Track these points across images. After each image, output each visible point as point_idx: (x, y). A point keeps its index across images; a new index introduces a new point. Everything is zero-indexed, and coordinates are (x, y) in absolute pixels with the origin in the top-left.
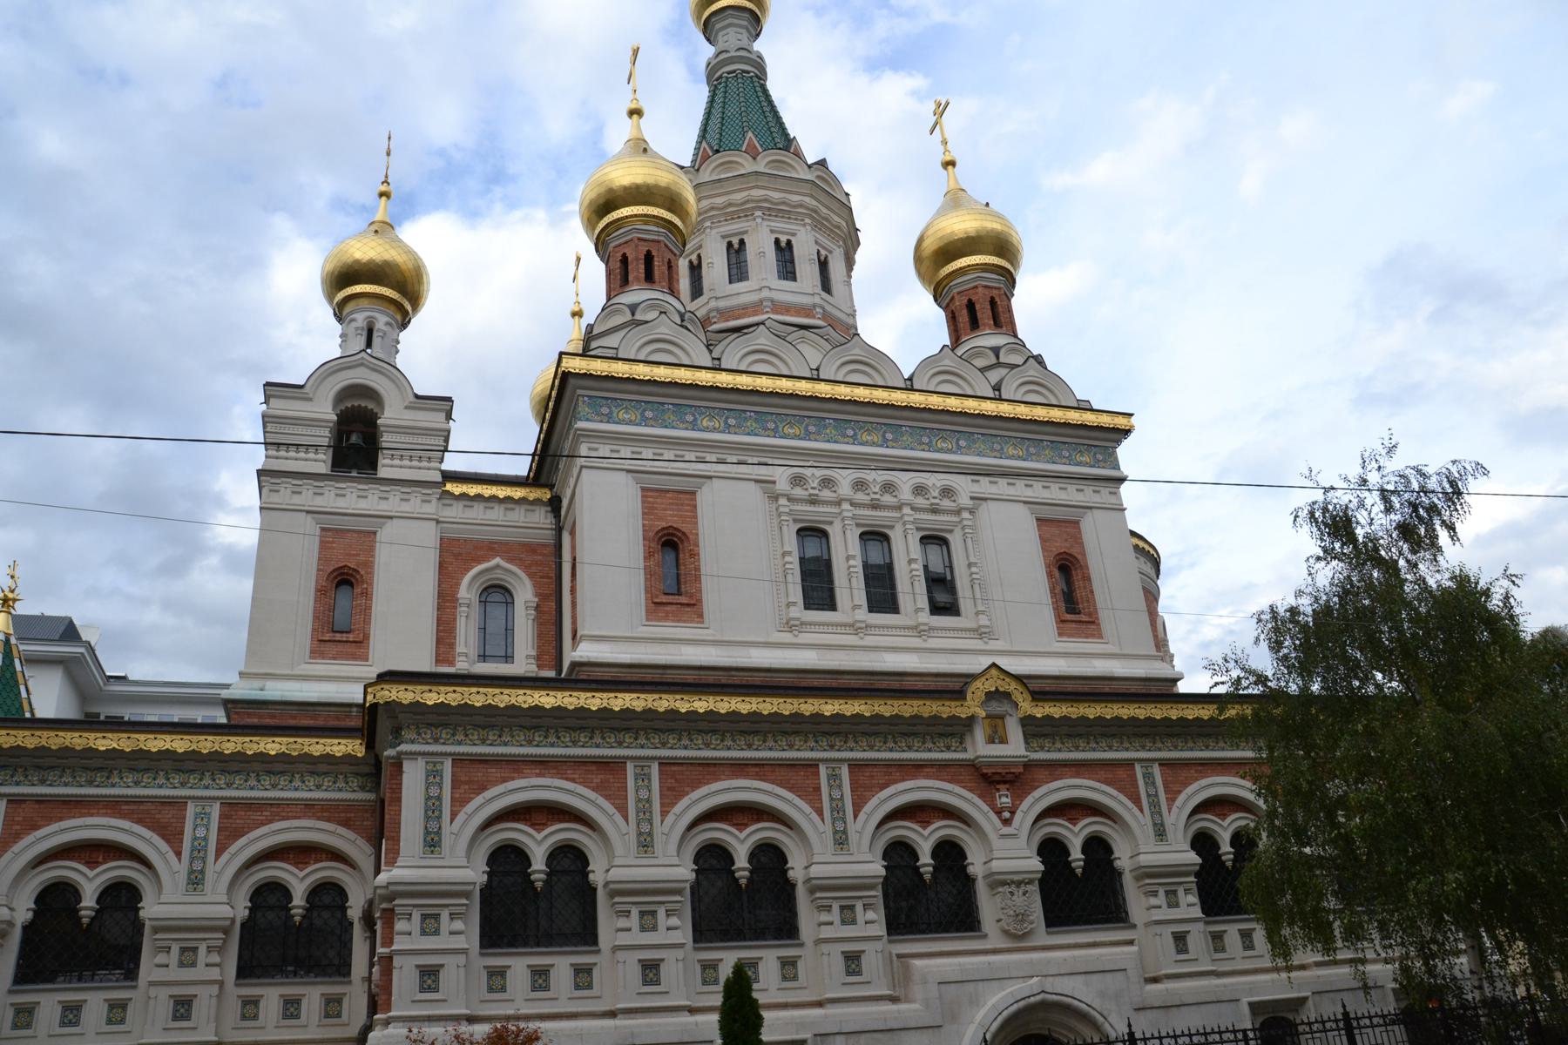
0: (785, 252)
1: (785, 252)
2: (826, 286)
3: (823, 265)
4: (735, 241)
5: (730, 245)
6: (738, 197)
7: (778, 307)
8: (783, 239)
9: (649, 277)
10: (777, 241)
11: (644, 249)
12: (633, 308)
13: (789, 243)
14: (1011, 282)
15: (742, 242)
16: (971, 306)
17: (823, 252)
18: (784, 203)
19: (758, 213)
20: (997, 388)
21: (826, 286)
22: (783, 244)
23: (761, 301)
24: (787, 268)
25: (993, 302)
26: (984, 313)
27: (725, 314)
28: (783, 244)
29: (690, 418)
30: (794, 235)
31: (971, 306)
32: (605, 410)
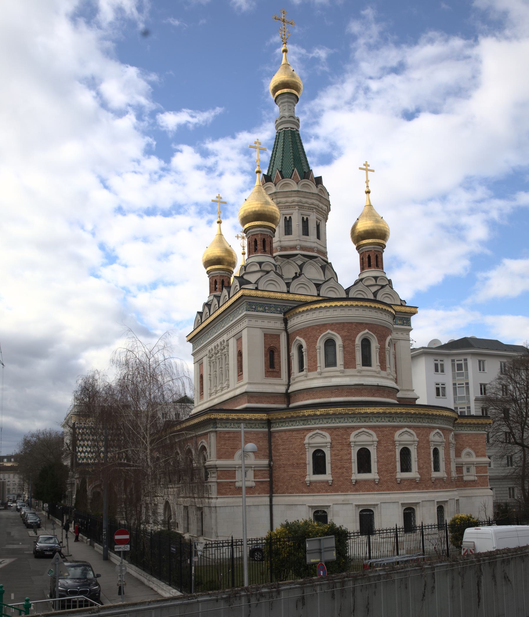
0: (305, 223)
1: (305, 223)
2: (318, 237)
3: (318, 226)
4: (288, 217)
5: (286, 218)
6: (290, 200)
7: (302, 248)
8: (305, 218)
9: (265, 251)
10: (303, 218)
11: (263, 237)
12: (260, 264)
13: (307, 218)
14: (384, 246)
15: (290, 217)
16: (369, 257)
17: (318, 221)
18: (306, 203)
19: (297, 207)
20: (375, 294)
21: (318, 237)
22: (305, 220)
23: (296, 245)
24: (306, 232)
25: (377, 257)
26: (373, 262)
27: (283, 248)
28: (305, 220)
29: (279, 309)
30: (309, 216)
31: (369, 257)
32: (254, 307)
